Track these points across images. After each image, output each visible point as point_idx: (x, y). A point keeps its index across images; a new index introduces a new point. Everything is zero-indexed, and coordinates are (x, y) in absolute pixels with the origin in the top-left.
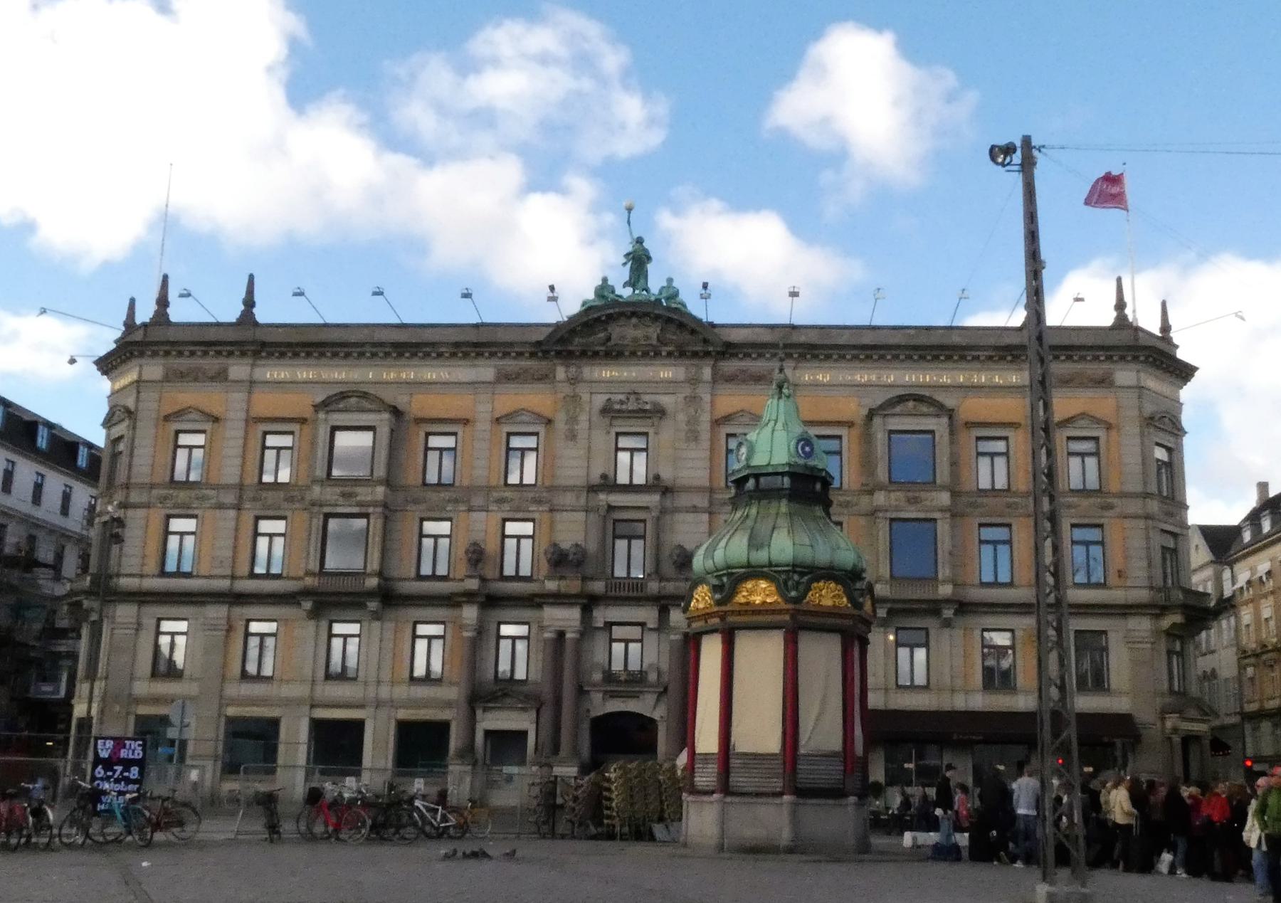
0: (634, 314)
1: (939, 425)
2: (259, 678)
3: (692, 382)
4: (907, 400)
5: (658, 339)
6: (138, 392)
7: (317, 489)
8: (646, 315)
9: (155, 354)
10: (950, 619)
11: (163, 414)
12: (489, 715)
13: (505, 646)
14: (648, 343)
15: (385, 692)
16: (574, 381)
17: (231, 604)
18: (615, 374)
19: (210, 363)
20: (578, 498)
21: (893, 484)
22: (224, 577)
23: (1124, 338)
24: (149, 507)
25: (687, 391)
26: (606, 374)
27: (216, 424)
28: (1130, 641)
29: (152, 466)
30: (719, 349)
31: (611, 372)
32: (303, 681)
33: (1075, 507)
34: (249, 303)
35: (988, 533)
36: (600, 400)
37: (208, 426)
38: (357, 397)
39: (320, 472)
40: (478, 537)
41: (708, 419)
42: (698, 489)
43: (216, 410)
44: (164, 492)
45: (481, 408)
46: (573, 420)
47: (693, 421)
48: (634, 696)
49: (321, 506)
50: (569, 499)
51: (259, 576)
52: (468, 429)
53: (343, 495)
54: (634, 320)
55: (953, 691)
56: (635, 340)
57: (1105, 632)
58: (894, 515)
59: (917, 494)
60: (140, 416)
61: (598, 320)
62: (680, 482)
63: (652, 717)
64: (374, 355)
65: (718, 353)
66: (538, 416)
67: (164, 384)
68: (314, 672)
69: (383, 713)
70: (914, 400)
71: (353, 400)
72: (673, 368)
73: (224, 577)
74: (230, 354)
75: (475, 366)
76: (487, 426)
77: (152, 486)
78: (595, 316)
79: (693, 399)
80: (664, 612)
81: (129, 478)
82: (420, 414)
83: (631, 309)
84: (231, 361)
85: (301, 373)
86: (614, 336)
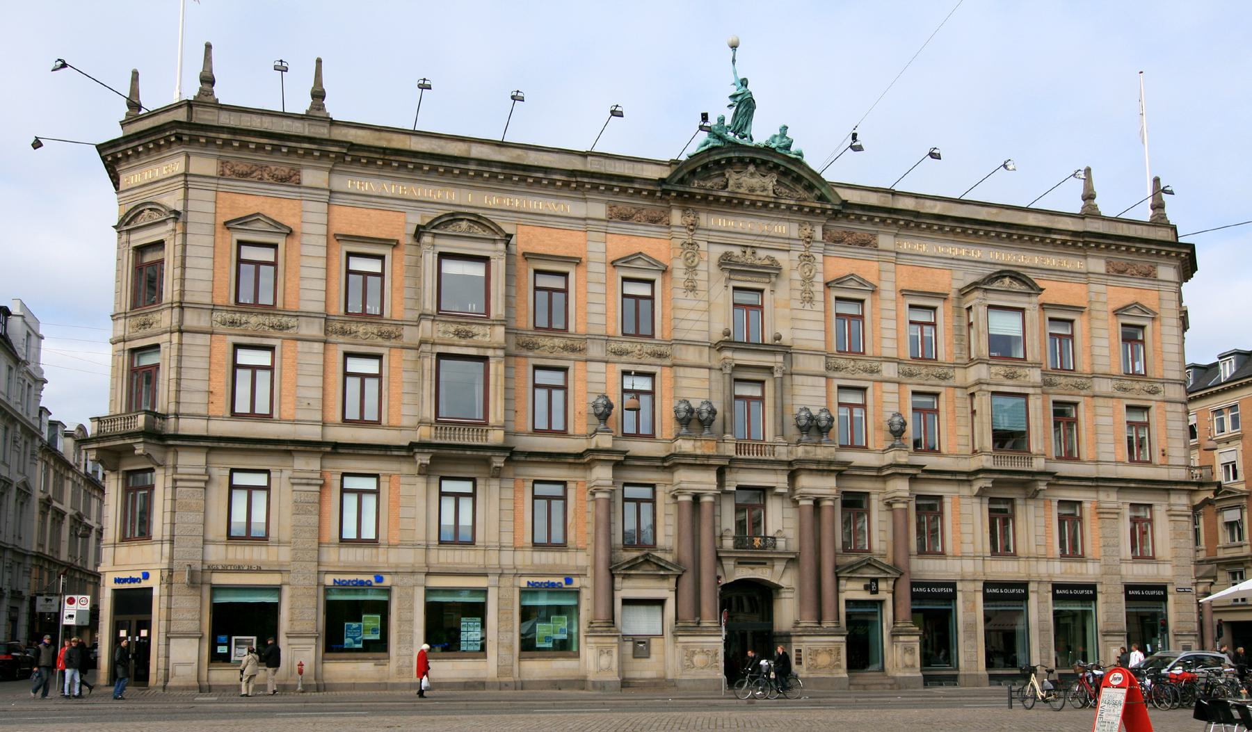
0: (753, 161)
1: (495, 251)
2: (359, 542)
3: (691, 227)
4: (1005, 277)
5: (774, 192)
6: (187, 188)
7: (427, 324)
8: (765, 163)
9: (211, 142)
10: (500, 467)
11: (222, 220)
12: (628, 583)
13: (350, 501)
14: (764, 194)
15: (507, 558)
16: (693, 227)
17: (325, 455)
18: (941, 249)
19: (279, 164)
20: (701, 353)
21: (440, 313)
22: (314, 423)
23: (1162, 234)
24: (212, 333)
25: (800, 247)
26: (722, 224)
27: (289, 239)
28: (1171, 514)
29: (897, 339)
30: (836, 207)
31: (727, 223)
32: (414, 546)
33: (627, 353)
34: (208, 80)
35: (543, 377)
36: (718, 251)
37: (281, 241)
38: (468, 220)
39: (430, 306)
40: (601, 389)
41: (822, 280)
42: (815, 353)
43: (289, 221)
44: (228, 316)
45: (592, 246)
46: (691, 269)
47: (807, 280)
48: (761, 563)
49: (433, 344)
50: (690, 355)
51: (242, 416)
52: (580, 269)
53: (458, 333)
54: (751, 168)
55: (501, 548)
56: (752, 190)
57: (1080, 503)
58: (994, 389)
59: (467, 328)
60: (191, 217)
61: (717, 162)
62: (797, 344)
63: (780, 584)
64: (479, 174)
65: (836, 212)
66: (654, 264)
67: (221, 182)
68: (427, 534)
69: (506, 582)
70: (1011, 277)
71: (464, 224)
72: (788, 224)
73: (314, 423)
74: (309, 152)
75: (585, 200)
76: (893, 295)
77: (213, 308)
78: (717, 158)
79: (807, 258)
80: (793, 476)
81: (182, 292)
82: (530, 249)
83: (751, 155)
84: (881, 228)
85: (390, 188)
86: (731, 182)
